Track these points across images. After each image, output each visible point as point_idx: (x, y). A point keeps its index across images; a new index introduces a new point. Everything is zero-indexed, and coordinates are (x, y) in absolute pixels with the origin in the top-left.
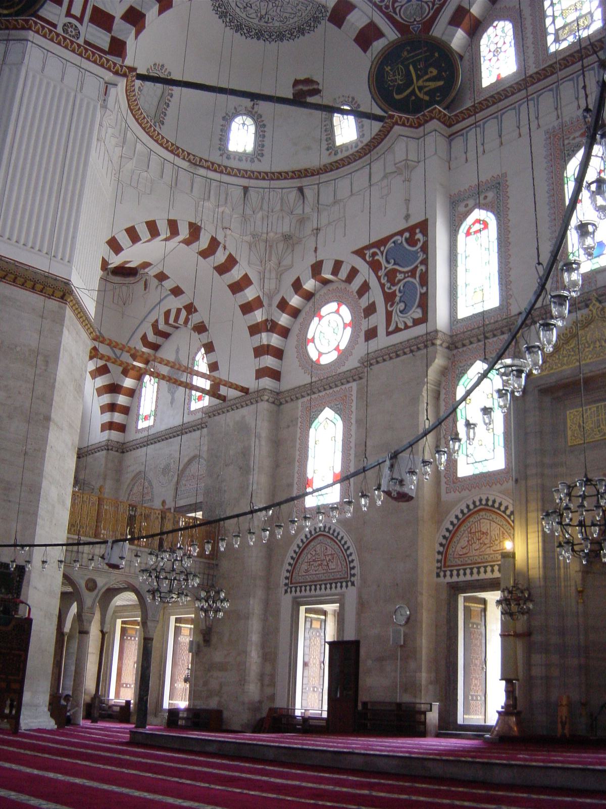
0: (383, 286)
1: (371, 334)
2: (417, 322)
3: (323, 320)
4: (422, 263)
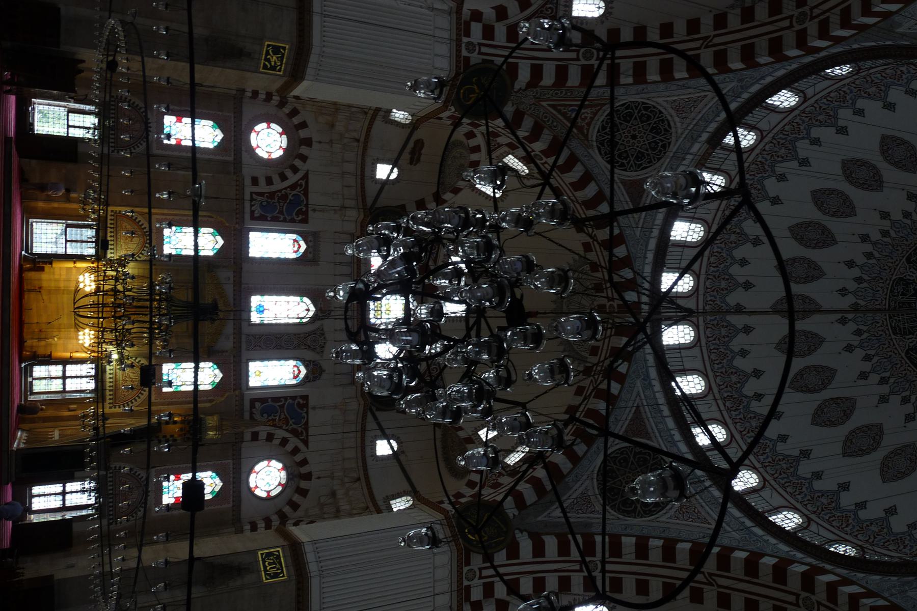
0: (280, 191)
1: (255, 181)
3: (279, 135)
4: (285, 218)
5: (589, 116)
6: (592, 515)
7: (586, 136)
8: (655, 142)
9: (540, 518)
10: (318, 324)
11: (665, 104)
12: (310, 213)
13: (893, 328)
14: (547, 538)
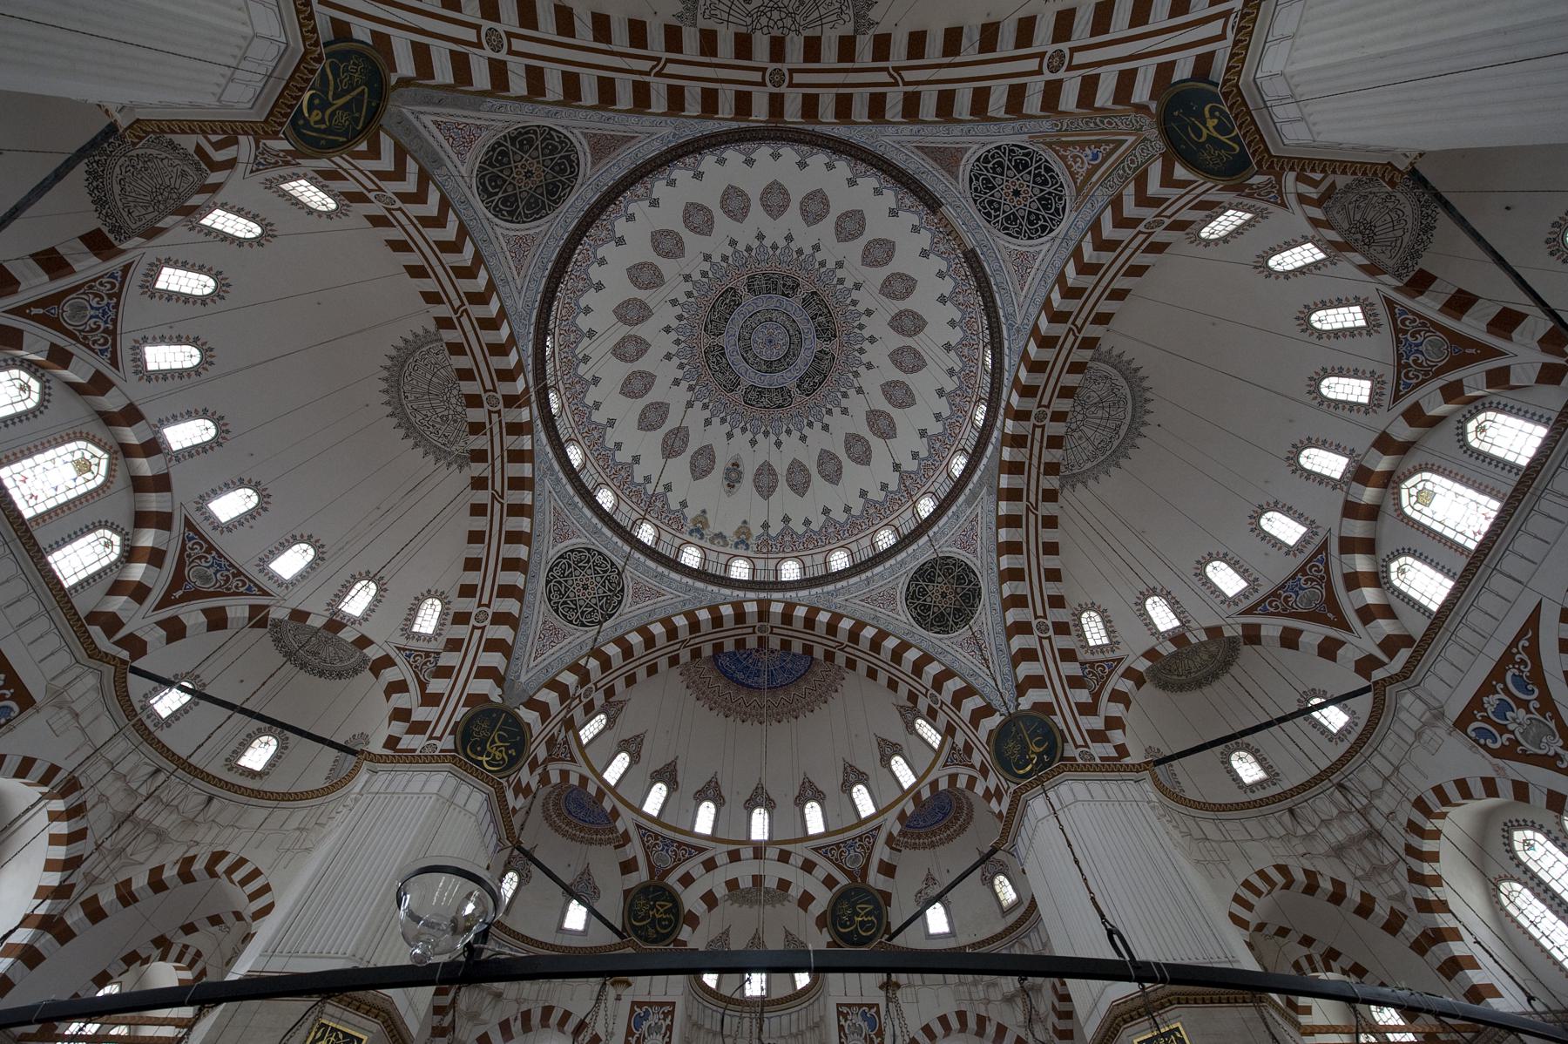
5: (1075, 167)
6: (454, 157)
7: (1050, 145)
8: (999, 209)
11: (1037, 249)
13: (753, 277)
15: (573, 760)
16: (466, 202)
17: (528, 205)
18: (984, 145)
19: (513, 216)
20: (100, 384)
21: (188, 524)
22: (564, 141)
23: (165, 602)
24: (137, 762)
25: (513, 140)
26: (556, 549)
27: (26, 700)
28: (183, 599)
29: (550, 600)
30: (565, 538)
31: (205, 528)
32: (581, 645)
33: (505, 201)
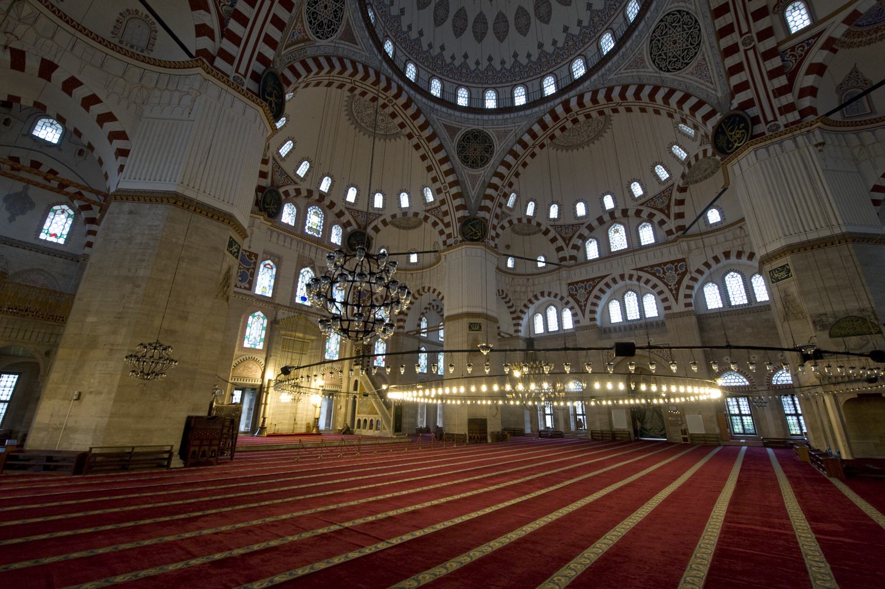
2: (245, 288)
4: (253, 268)
7: (309, 40)
9: (473, 202)
10: (317, 269)
12: (250, 250)
14: (483, 204)
15: (819, 35)
16: (493, 166)
17: (485, 142)
18: (332, 42)
19: (491, 146)
20: (590, 228)
21: (642, 204)
22: (459, 146)
23: (668, 216)
24: (729, 234)
25: (467, 163)
26: (649, 66)
27: (683, 260)
28: (669, 211)
29: (680, 69)
30: (643, 60)
31: (643, 200)
32: (712, 47)
33: (487, 152)
